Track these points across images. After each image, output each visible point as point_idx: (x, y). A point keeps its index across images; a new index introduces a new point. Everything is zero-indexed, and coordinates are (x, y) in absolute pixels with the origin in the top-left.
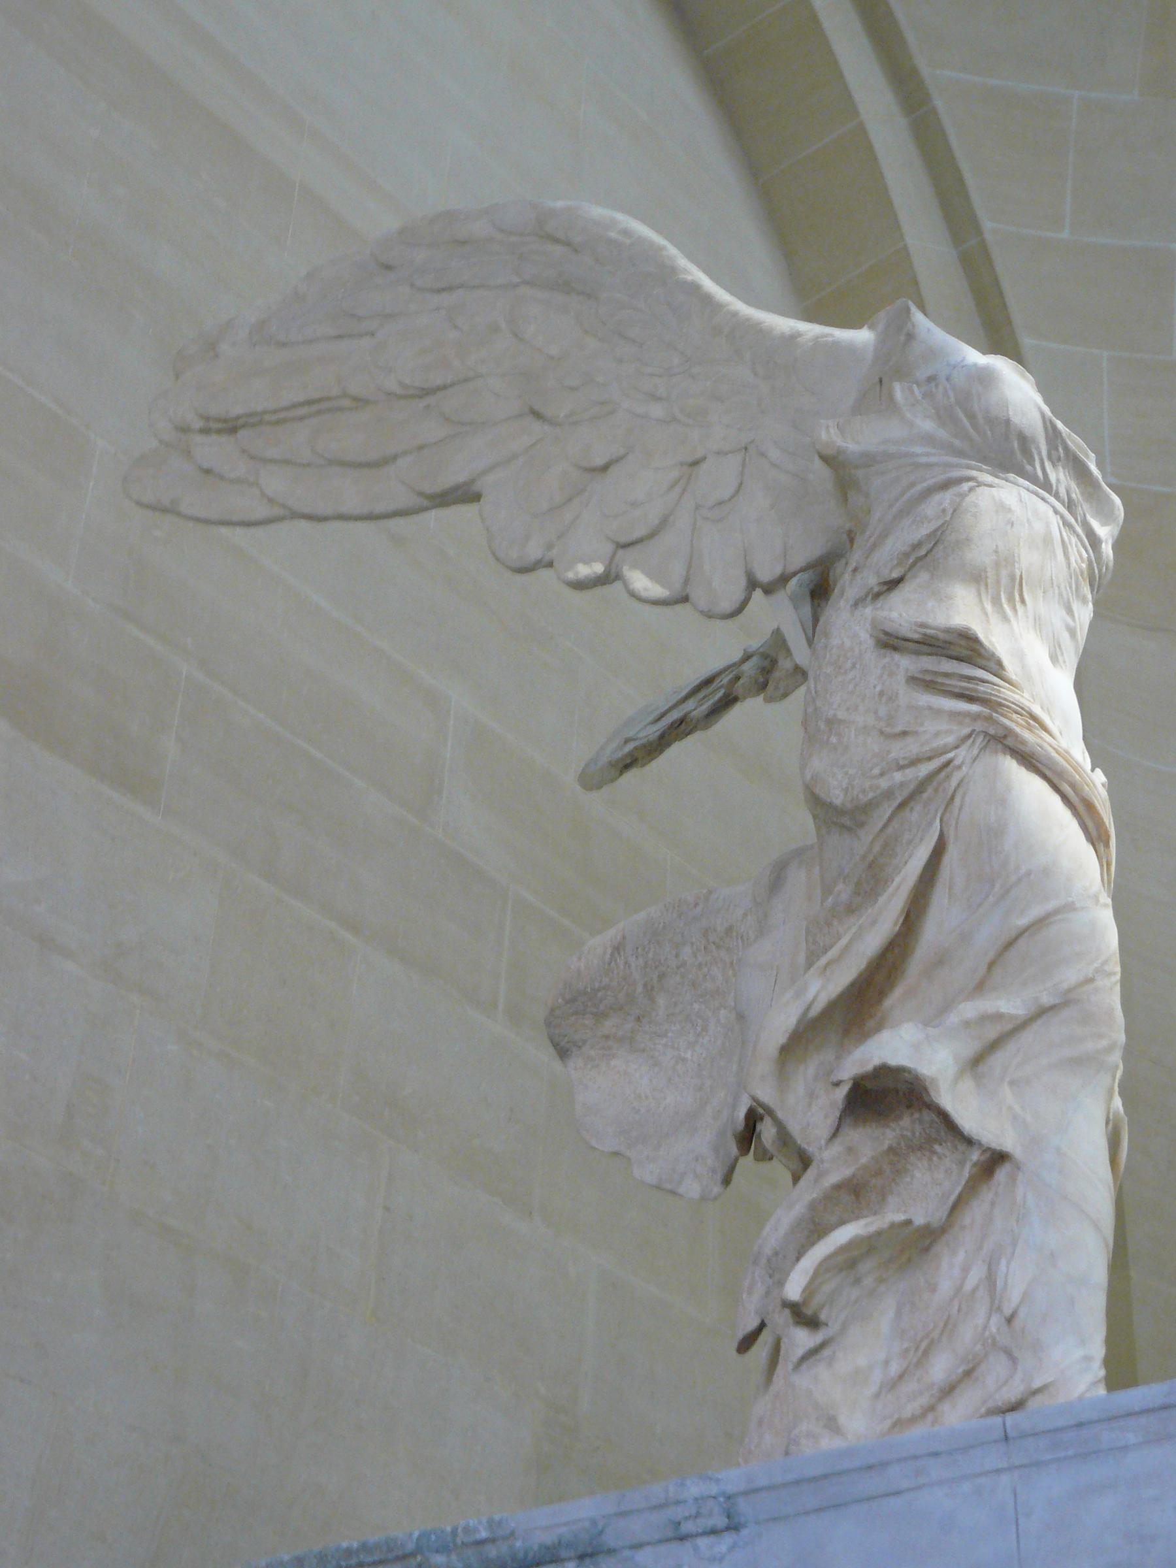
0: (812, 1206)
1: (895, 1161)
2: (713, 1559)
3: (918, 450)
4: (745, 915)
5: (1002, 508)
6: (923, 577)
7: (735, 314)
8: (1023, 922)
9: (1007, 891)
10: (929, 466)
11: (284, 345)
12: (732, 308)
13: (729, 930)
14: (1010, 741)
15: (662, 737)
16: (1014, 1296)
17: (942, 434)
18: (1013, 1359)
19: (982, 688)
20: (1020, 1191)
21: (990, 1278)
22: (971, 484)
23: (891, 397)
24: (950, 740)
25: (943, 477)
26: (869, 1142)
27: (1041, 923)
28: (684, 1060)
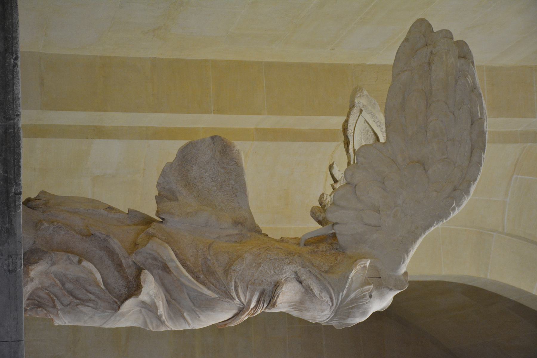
0: (118, 254)
1: (125, 278)
2: (2, 265)
3: (345, 292)
4: (239, 203)
5: (323, 311)
6: (303, 290)
7: (420, 235)
8: (185, 314)
9: (194, 311)
10: (338, 295)
11: (456, 82)
12: (423, 234)
13: (236, 196)
14: (241, 312)
15: (347, 137)
16: (82, 308)
17: (349, 299)
18: (67, 306)
19: (261, 306)
20: (109, 311)
21: (90, 300)
22: (331, 304)
23: (369, 284)
24: (243, 300)
25: (334, 298)
26: (130, 272)
27: (185, 319)
28: (206, 173)
